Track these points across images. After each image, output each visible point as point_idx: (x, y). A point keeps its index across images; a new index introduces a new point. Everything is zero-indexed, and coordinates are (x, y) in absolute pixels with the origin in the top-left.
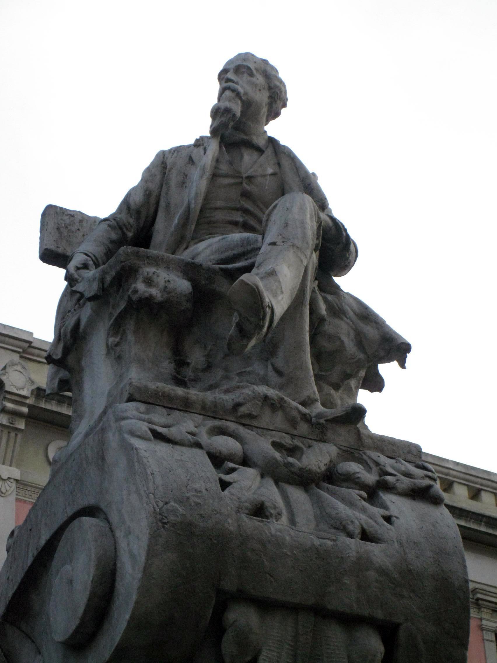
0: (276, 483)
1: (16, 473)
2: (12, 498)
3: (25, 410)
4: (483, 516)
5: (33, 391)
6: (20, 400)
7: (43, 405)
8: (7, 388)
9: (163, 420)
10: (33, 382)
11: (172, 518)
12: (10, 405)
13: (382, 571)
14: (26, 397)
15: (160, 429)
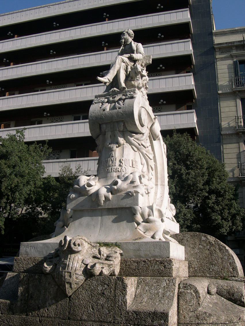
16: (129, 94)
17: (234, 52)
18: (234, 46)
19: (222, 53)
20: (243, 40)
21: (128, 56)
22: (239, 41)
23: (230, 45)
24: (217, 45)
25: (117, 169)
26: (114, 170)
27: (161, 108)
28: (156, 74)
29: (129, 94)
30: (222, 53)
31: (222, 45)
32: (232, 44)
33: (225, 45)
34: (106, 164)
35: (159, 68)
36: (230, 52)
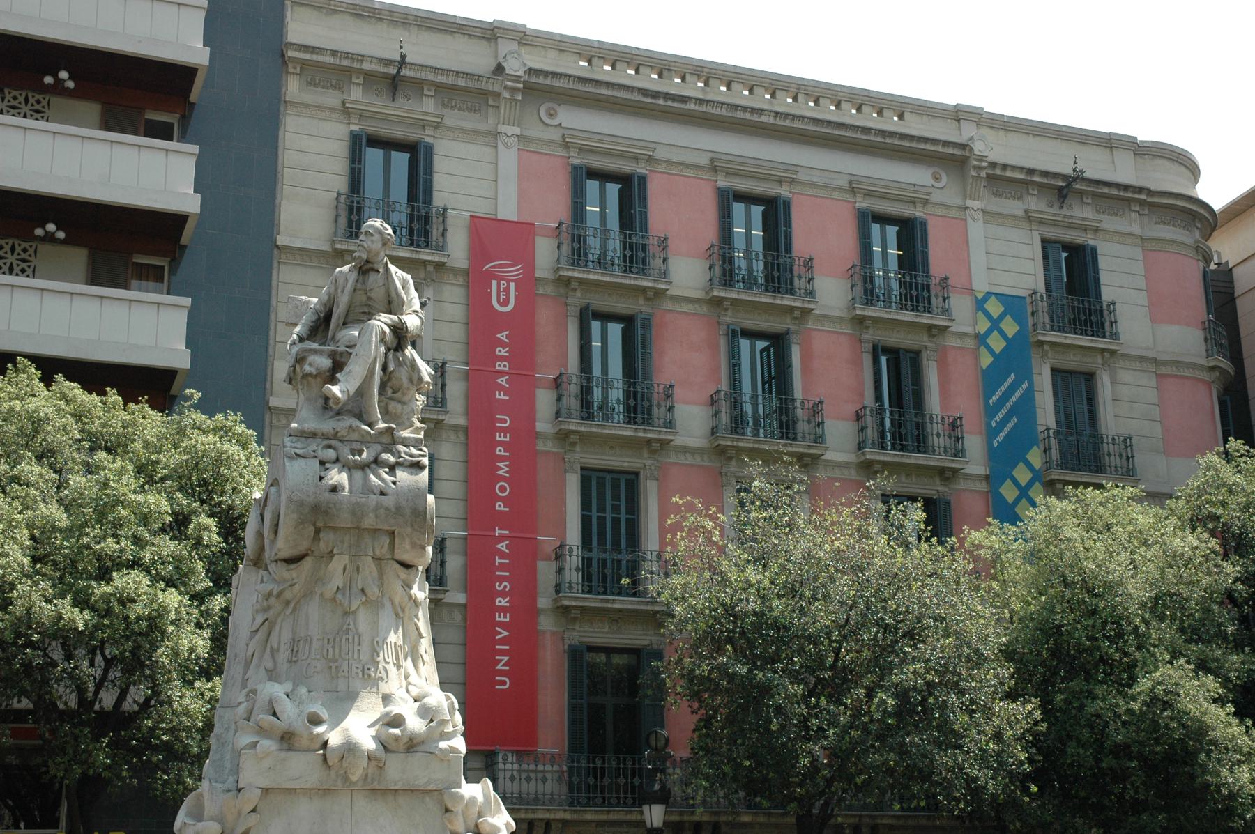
0: (349, 469)
1: (517, 130)
2: (515, 149)
3: (521, 86)
4: (858, 127)
5: (525, 72)
6: (516, 79)
7: (533, 79)
8: (507, 71)
9: (302, 446)
10: (525, 65)
11: (295, 499)
12: (509, 83)
13: (387, 509)
14: (521, 77)
15: (299, 452)
16: (406, 453)
17: (356, 94)
18: (359, 71)
19: (312, 88)
20: (398, 58)
21: (389, 322)
22: (381, 61)
23: (346, 63)
24: (296, 50)
25: (366, 671)
26: (357, 673)
27: (31, 251)
28: (24, 96)
29: (406, 453)
30: (309, 84)
31: (317, 54)
32: (356, 65)
33: (328, 59)
34: (331, 650)
35: (48, 80)
36: (340, 88)
